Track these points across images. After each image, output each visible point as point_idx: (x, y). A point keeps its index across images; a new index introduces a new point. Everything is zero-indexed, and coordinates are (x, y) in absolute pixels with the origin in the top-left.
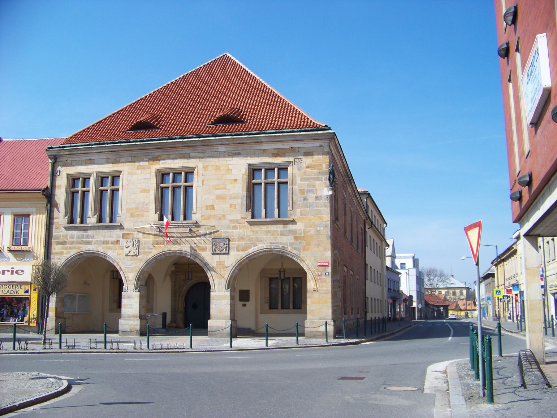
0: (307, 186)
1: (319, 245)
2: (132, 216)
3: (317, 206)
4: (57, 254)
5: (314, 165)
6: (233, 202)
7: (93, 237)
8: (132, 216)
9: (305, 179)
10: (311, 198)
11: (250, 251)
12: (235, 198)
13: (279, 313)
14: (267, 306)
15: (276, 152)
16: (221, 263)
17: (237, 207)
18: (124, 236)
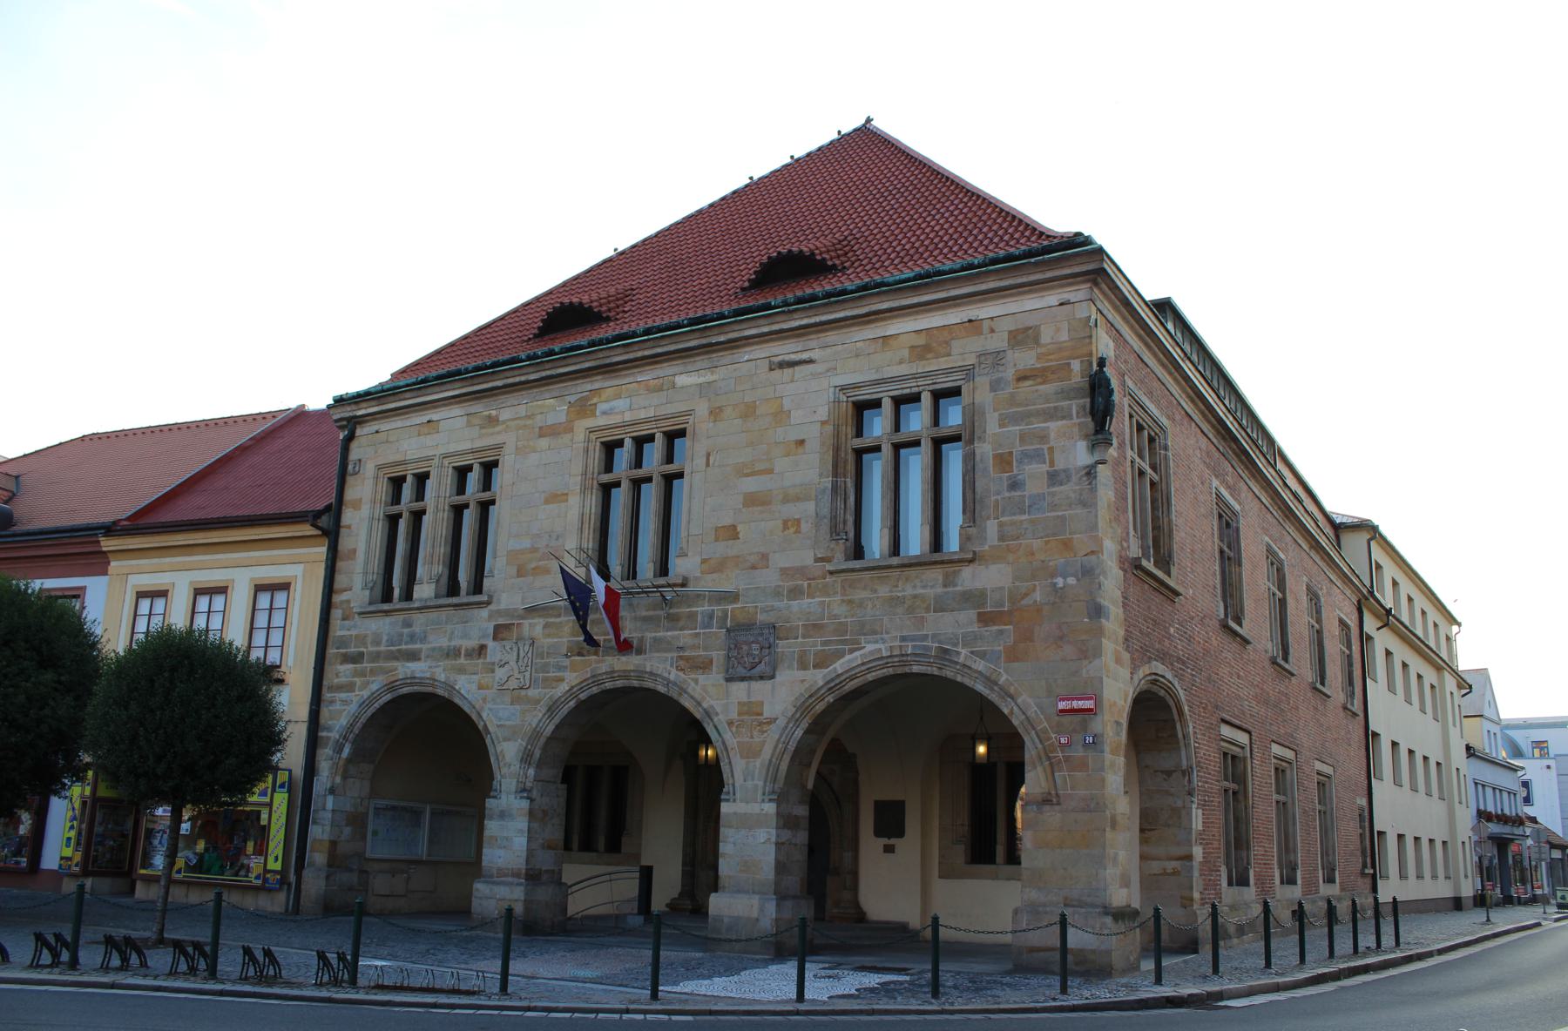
1: (1061, 638)
2: (520, 573)
3: (1054, 507)
4: (340, 688)
5: (1044, 369)
6: (793, 510)
7: (423, 640)
8: (520, 573)
11: (839, 666)
12: (798, 499)
13: (995, 877)
14: (959, 853)
15: (921, 340)
16: (751, 709)
17: (804, 527)
18: (499, 632)
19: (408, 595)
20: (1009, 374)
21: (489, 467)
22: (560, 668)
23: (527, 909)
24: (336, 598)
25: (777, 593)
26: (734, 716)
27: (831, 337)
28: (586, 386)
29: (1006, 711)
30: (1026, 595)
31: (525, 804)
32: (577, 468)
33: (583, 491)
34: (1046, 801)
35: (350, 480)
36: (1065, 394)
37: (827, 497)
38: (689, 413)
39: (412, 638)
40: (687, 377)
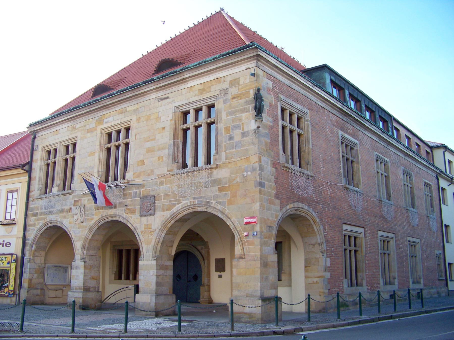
0: (233, 121)
1: (246, 195)
3: (244, 145)
4: (32, 225)
5: (241, 94)
6: (161, 153)
10: (237, 134)
11: (174, 210)
15: (201, 87)
16: (148, 226)
17: (165, 159)
20: (229, 97)
22: (93, 215)
23: (83, 301)
24: (31, 194)
25: (156, 184)
26: (143, 229)
27: (174, 89)
28: (100, 113)
29: (228, 224)
30: (234, 179)
31: (83, 263)
32: (98, 143)
33: (100, 150)
34: (241, 257)
35: (35, 153)
36: (247, 103)
37: (172, 147)
38: (130, 120)
40: (130, 106)
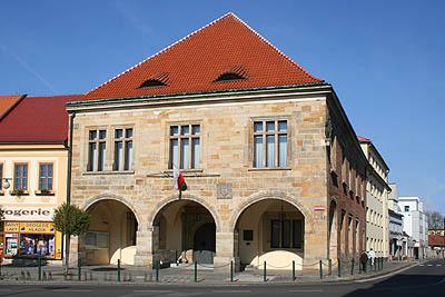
2: (144, 165)
6: (237, 152)
9: (303, 132)
10: (309, 148)
11: (252, 196)
16: (225, 209)
19: (100, 169)
21: (129, 131)
25: (232, 175)
34: (311, 232)
39: (105, 183)
